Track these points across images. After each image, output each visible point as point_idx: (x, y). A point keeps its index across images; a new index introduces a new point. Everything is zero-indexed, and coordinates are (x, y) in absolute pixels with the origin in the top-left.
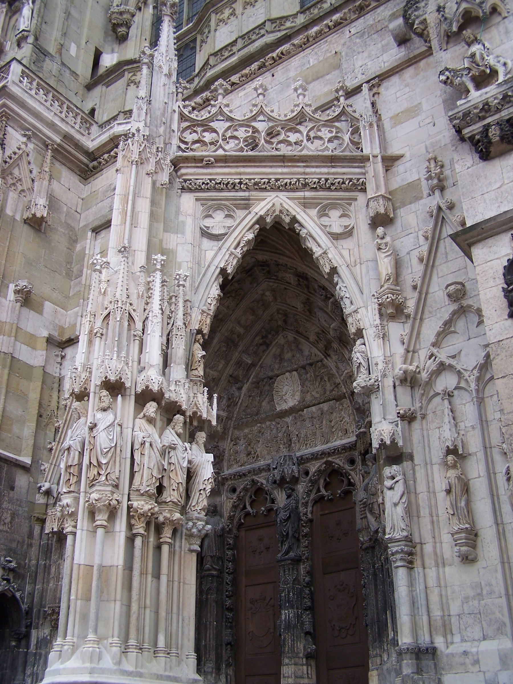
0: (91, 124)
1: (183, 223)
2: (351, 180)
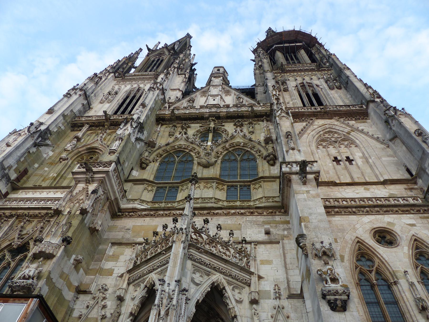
0: (124, 197)
1: (187, 272)
2: (246, 280)
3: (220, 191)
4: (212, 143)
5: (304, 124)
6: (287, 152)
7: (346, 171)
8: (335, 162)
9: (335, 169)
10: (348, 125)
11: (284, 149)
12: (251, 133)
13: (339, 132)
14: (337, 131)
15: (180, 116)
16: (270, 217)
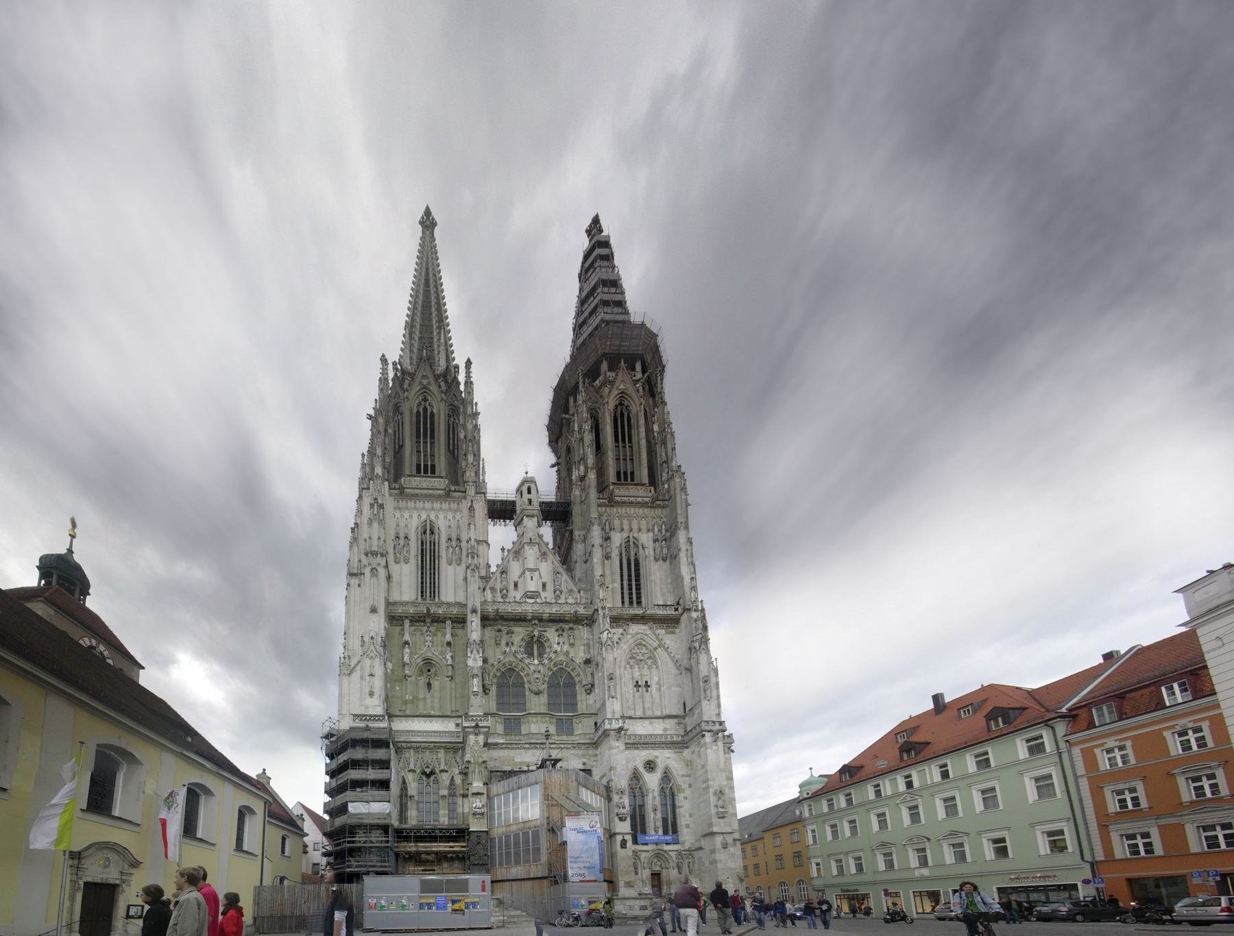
5: (621, 630)
8: (635, 689)
9: (634, 696)
10: (657, 636)
13: (648, 645)
15: (503, 616)
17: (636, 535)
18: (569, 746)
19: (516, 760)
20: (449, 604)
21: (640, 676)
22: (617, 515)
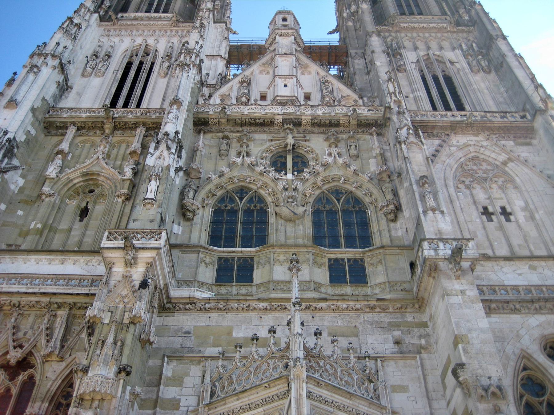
3: (319, 268)
4: (293, 175)
5: (437, 142)
6: (425, 212)
7: (501, 232)
9: (484, 228)
11: (421, 209)
12: (354, 158)
13: (490, 159)
14: (487, 158)
16: (399, 315)
17: (437, 53)
18: (358, 306)
19: (234, 335)
20: (148, 111)
21: (489, 198)
22: (407, 38)
